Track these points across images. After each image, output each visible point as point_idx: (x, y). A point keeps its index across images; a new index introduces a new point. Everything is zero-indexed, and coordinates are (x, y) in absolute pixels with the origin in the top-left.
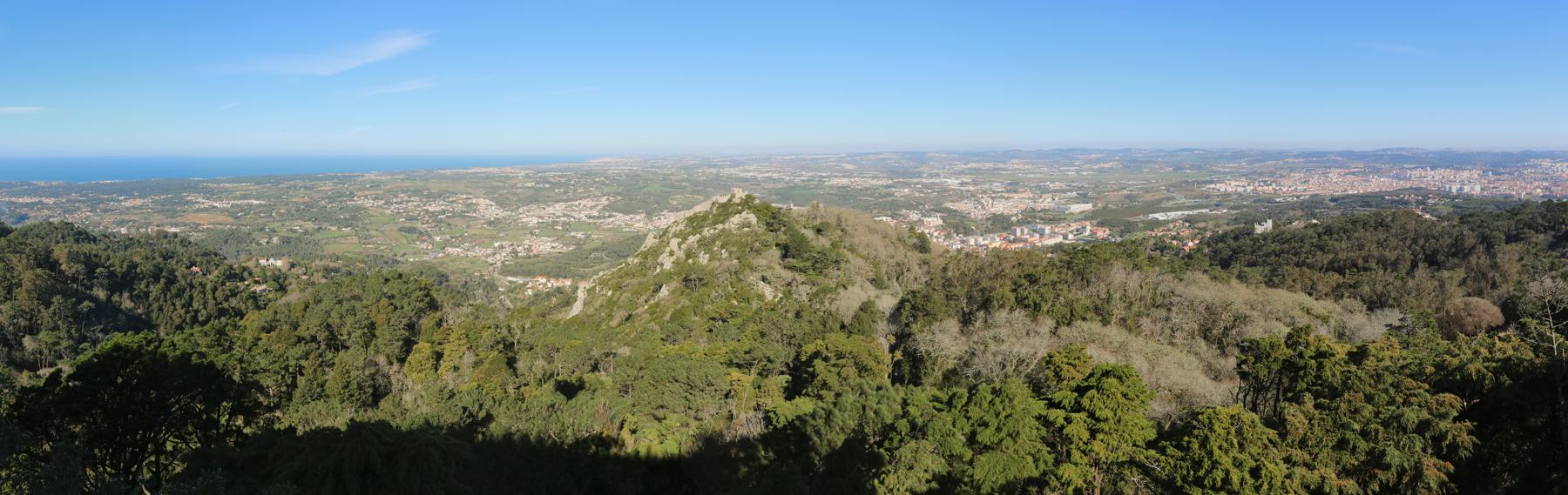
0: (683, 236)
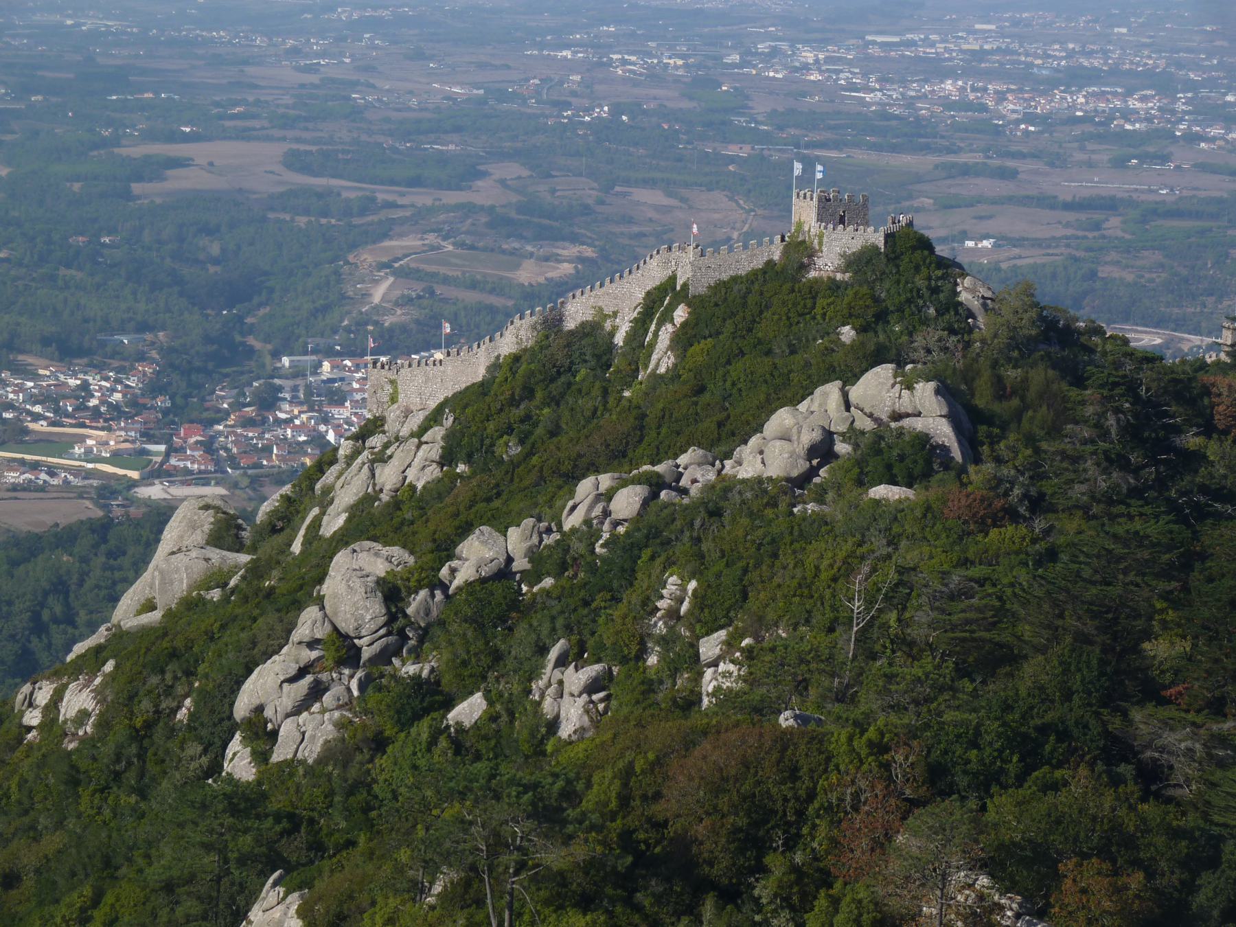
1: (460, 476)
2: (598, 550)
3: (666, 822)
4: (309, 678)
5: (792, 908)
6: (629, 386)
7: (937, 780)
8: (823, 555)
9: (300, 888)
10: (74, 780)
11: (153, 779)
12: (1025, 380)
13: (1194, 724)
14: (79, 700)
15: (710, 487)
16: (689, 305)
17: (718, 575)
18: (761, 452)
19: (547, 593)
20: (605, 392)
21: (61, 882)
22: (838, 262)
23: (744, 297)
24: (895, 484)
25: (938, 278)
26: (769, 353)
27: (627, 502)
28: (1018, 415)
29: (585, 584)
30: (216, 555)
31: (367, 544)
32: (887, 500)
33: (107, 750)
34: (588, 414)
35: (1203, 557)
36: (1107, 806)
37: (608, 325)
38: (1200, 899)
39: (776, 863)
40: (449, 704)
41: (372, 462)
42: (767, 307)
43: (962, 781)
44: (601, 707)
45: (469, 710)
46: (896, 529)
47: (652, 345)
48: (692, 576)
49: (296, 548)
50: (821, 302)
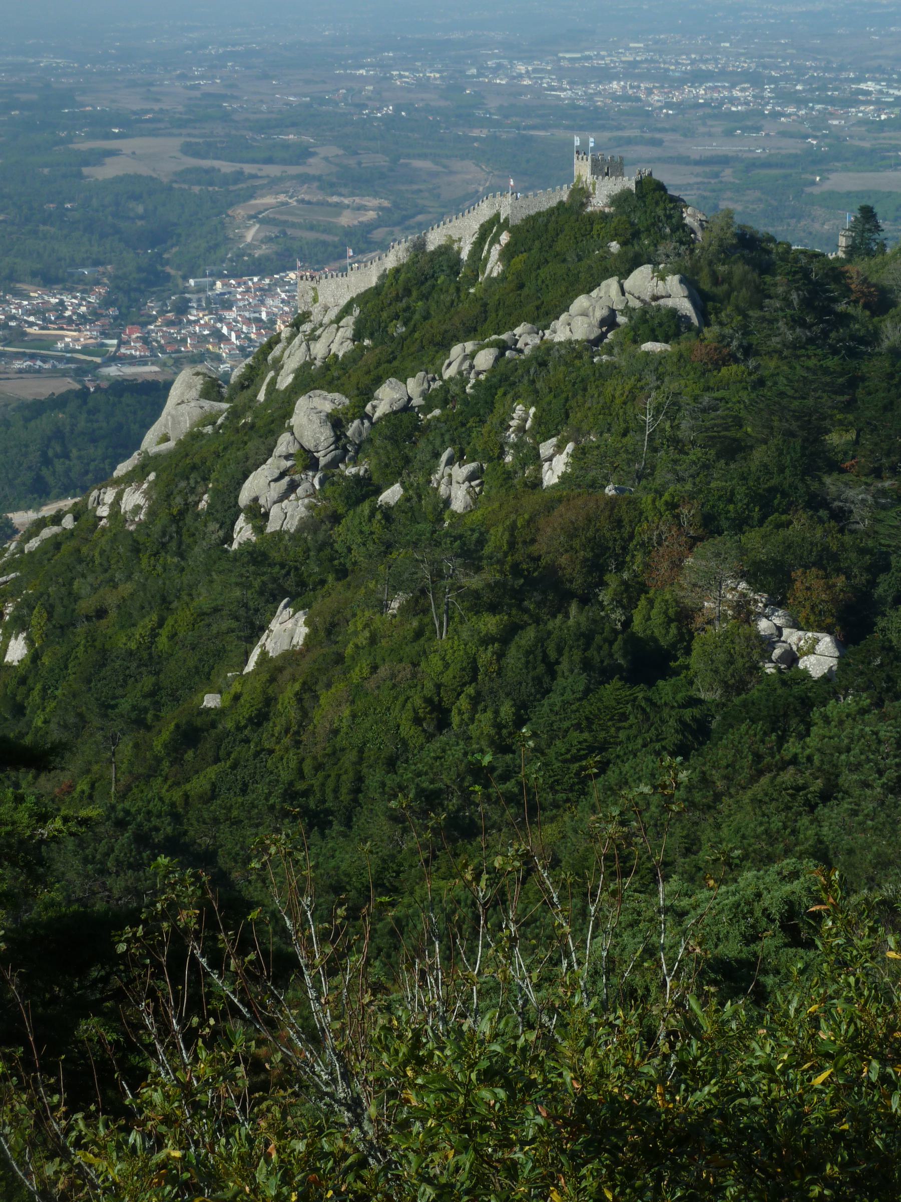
0: (350, 377)
1: (366, 347)
2: (468, 390)
3: (540, 556)
4: (287, 479)
5: (623, 607)
6: (473, 286)
7: (710, 525)
8: (615, 388)
9: (303, 608)
10: (136, 549)
11: (189, 546)
12: (730, 273)
13: (866, 484)
14: (133, 499)
15: (537, 348)
16: (510, 232)
17: (549, 403)
18: (569, 324)
19: (437, 419)
20: (458, 290)
21: (135, 613)
22: (608, 201)
23: (546, 225)
24: (657, 341)
25: (671, 209)
26: (564, 261)
27: (485, 359)
28: (728, 295)
29: (461, 413)
30: (207, 404)
31: (318, 392)
32: (653, 352)
33: (156, 529)
34: (448, 304)
35: (863, 379)
36: (818, 535)
37: (456, 247)
38: (879, 591)
39: (612, 580)
40: (378, 491)
41: (308, 340)
42: (562, 231)
43: (725, 524)
44: (477, 489)
45: (392, 494)
46: (661, 370)
47: (487, 259)
48: (532, 404)
49: (261, 397)
50: (596, 227)
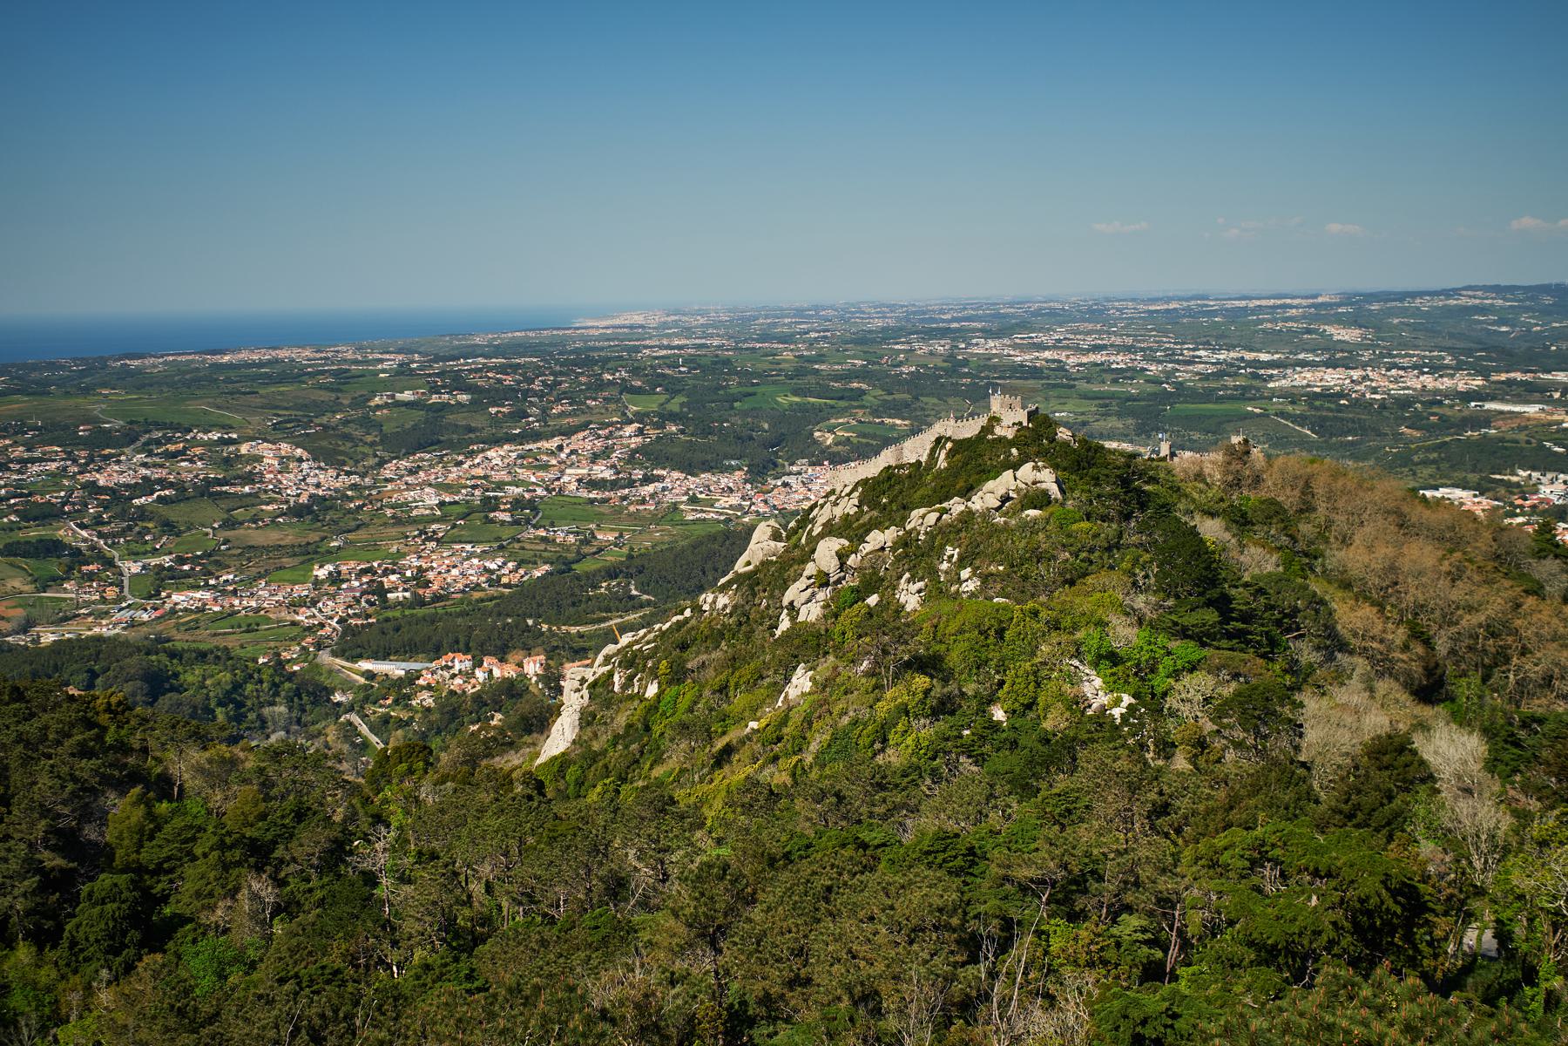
0: (851, 529)
14: (723, 600)
30: (772, 543)
45: (873, 600)
49: (803, 541)
